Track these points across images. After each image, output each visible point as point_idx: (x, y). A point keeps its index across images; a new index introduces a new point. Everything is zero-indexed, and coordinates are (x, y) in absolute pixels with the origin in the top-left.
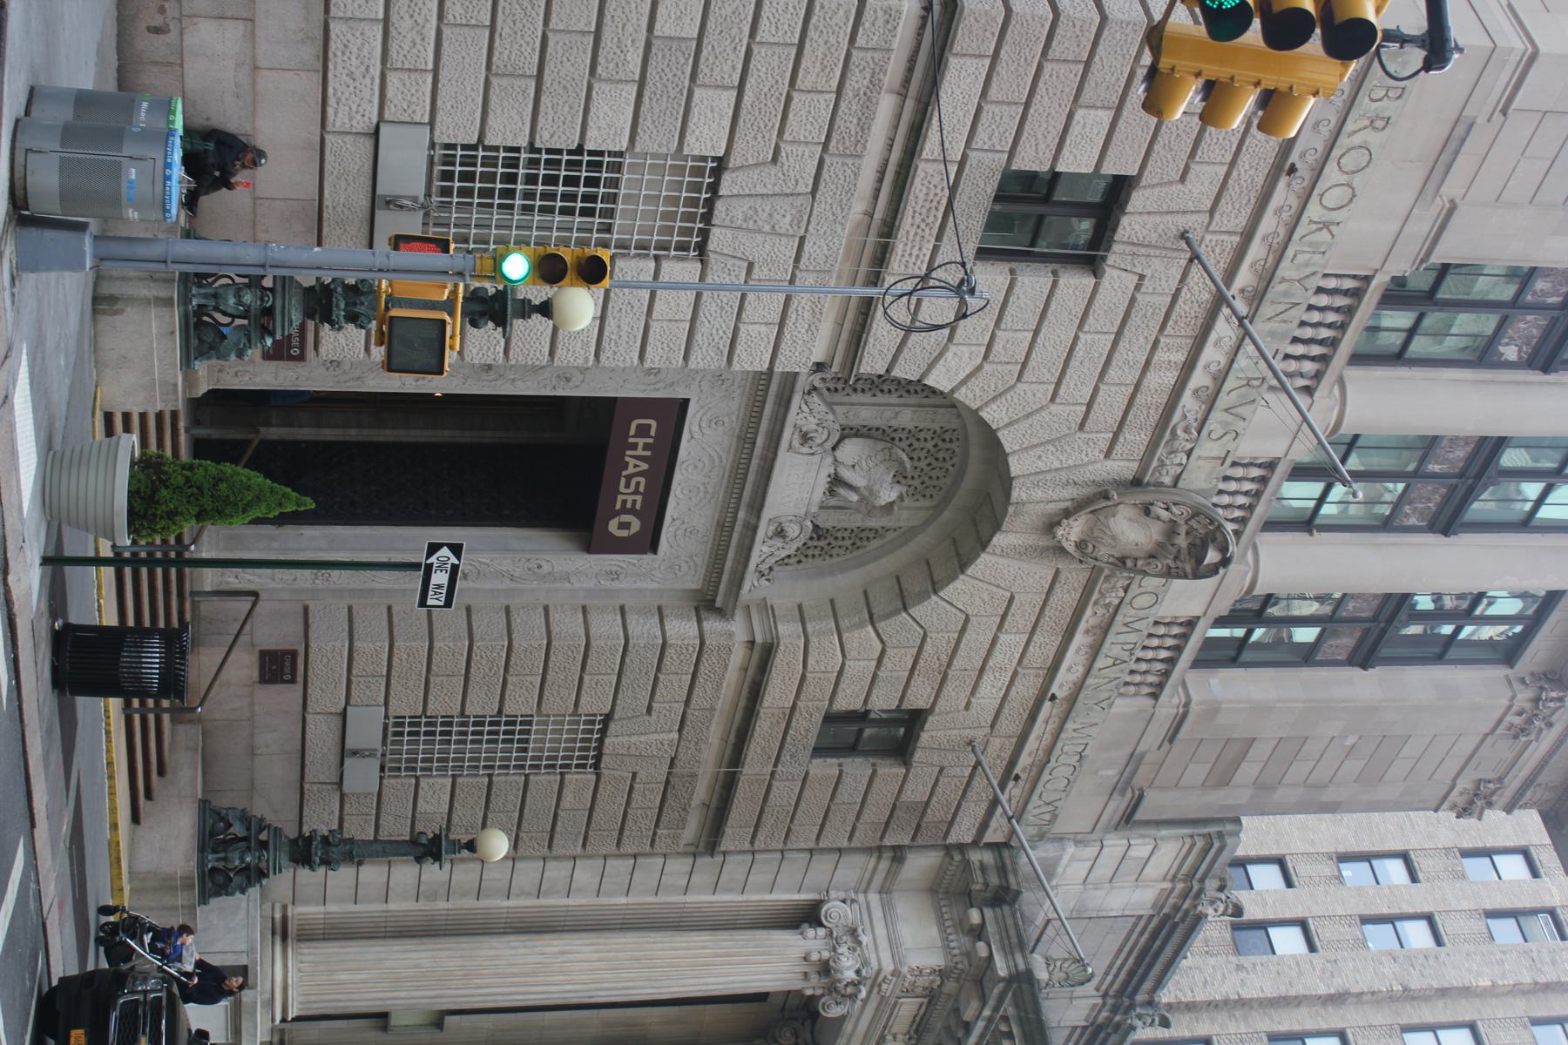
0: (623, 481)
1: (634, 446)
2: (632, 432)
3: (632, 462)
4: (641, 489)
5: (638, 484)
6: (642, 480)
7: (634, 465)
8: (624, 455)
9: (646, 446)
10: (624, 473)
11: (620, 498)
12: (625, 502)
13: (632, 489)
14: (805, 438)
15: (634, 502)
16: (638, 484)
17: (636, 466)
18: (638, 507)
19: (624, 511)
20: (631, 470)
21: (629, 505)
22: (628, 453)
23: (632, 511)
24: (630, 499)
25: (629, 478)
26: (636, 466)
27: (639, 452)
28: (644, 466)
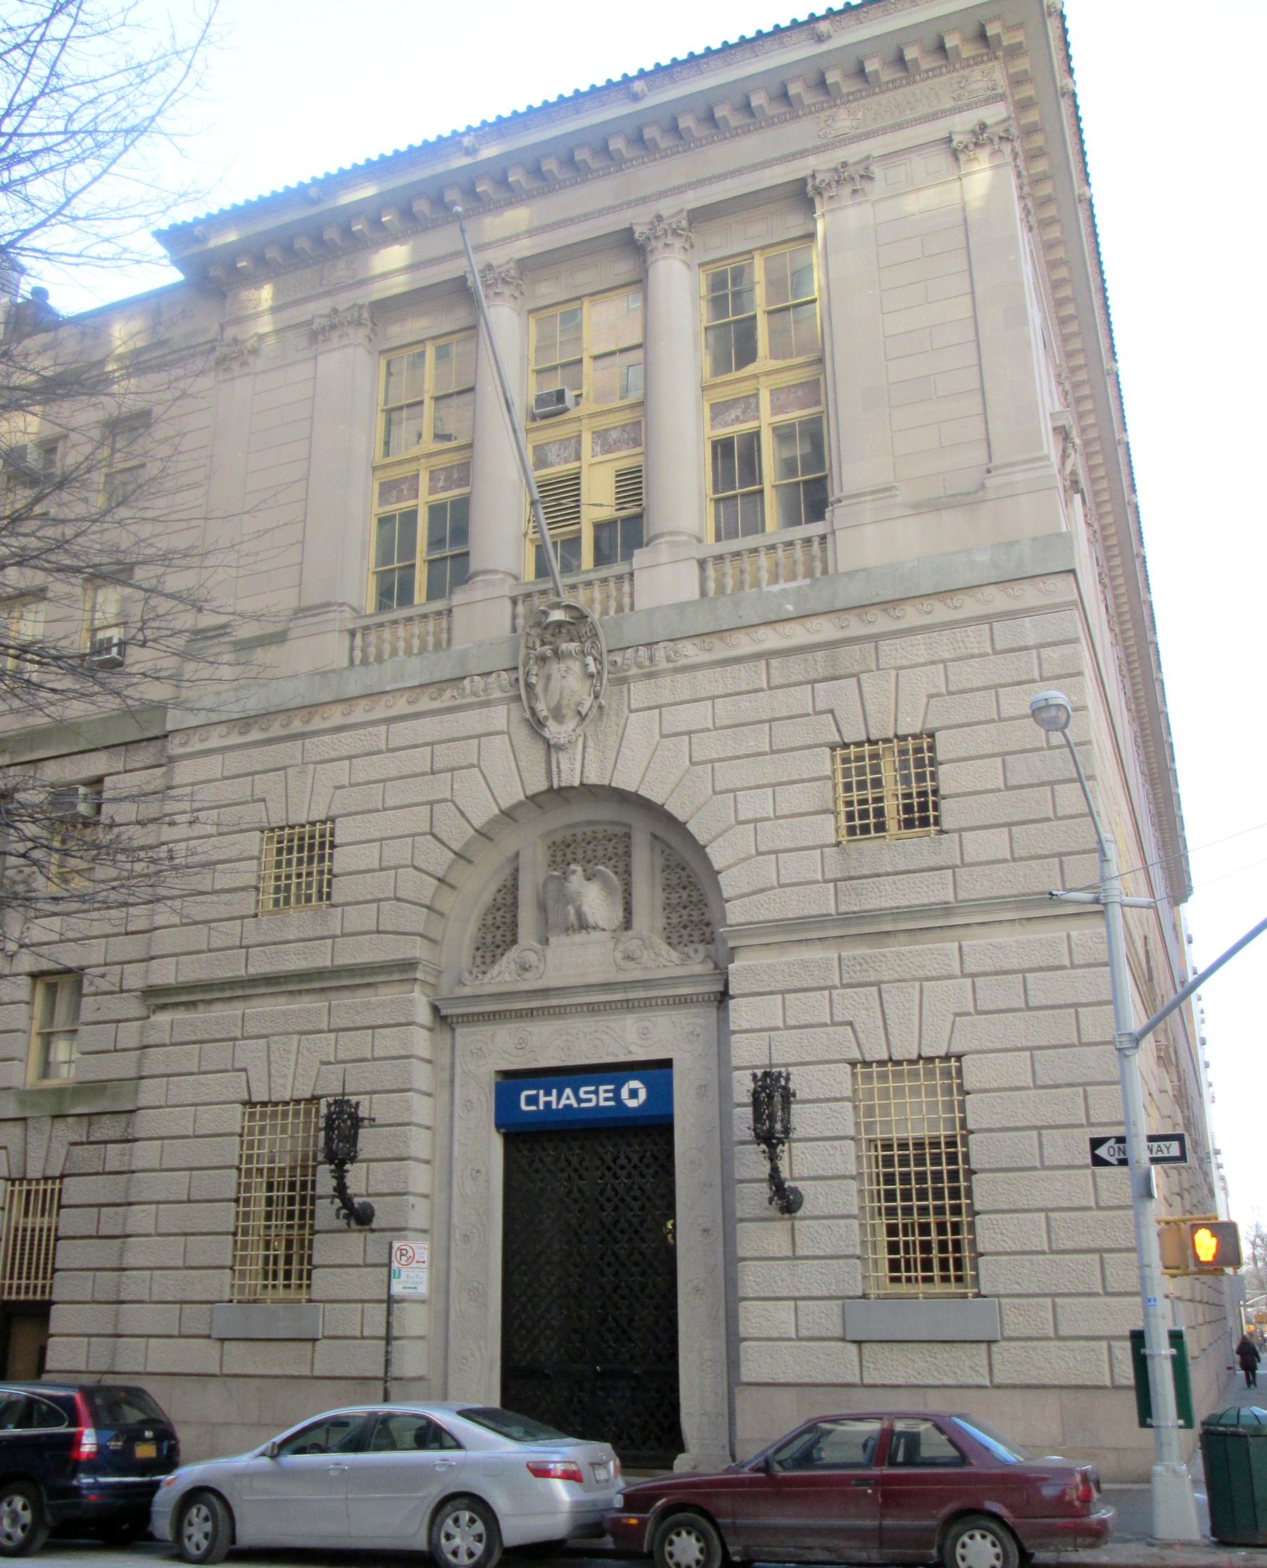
0: (583, 1105)
1: (548, 1104)
2: (533, 1108)
3: (564, 1102)
4: (592, 1088)
5: (586, 1093)
6: (583, 1089)
7: (568, 1097)
8: (557, 1110)
9: (548, 1093)
10: (575, 1105)
11: (602, 1103)
12: (606, 1099)
13: (593, 1096)
14: (525, 968)
15: (606, 1091)
16: (586, 1093)
17: (568, 1098)
18: (611, 1087)
19: (617, 1096)
20: (573, 1102)
21: (611, 1095)
22: (554, 1106)
23: (617, 1092)
24: (602, 1095)
25: (580, 1100)
26: (568, 1098)
27: (553, 1098)
28: (568, 1091)
